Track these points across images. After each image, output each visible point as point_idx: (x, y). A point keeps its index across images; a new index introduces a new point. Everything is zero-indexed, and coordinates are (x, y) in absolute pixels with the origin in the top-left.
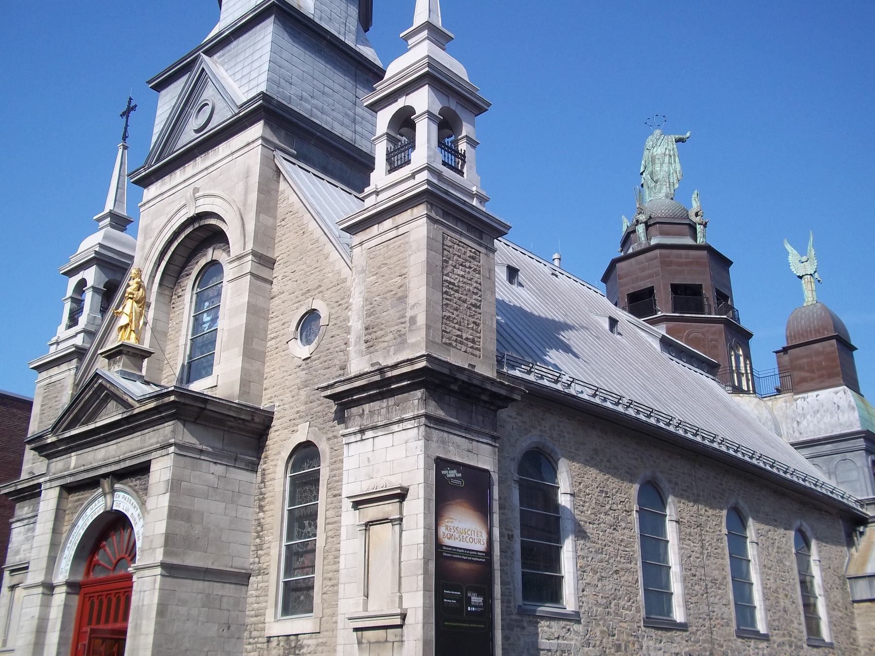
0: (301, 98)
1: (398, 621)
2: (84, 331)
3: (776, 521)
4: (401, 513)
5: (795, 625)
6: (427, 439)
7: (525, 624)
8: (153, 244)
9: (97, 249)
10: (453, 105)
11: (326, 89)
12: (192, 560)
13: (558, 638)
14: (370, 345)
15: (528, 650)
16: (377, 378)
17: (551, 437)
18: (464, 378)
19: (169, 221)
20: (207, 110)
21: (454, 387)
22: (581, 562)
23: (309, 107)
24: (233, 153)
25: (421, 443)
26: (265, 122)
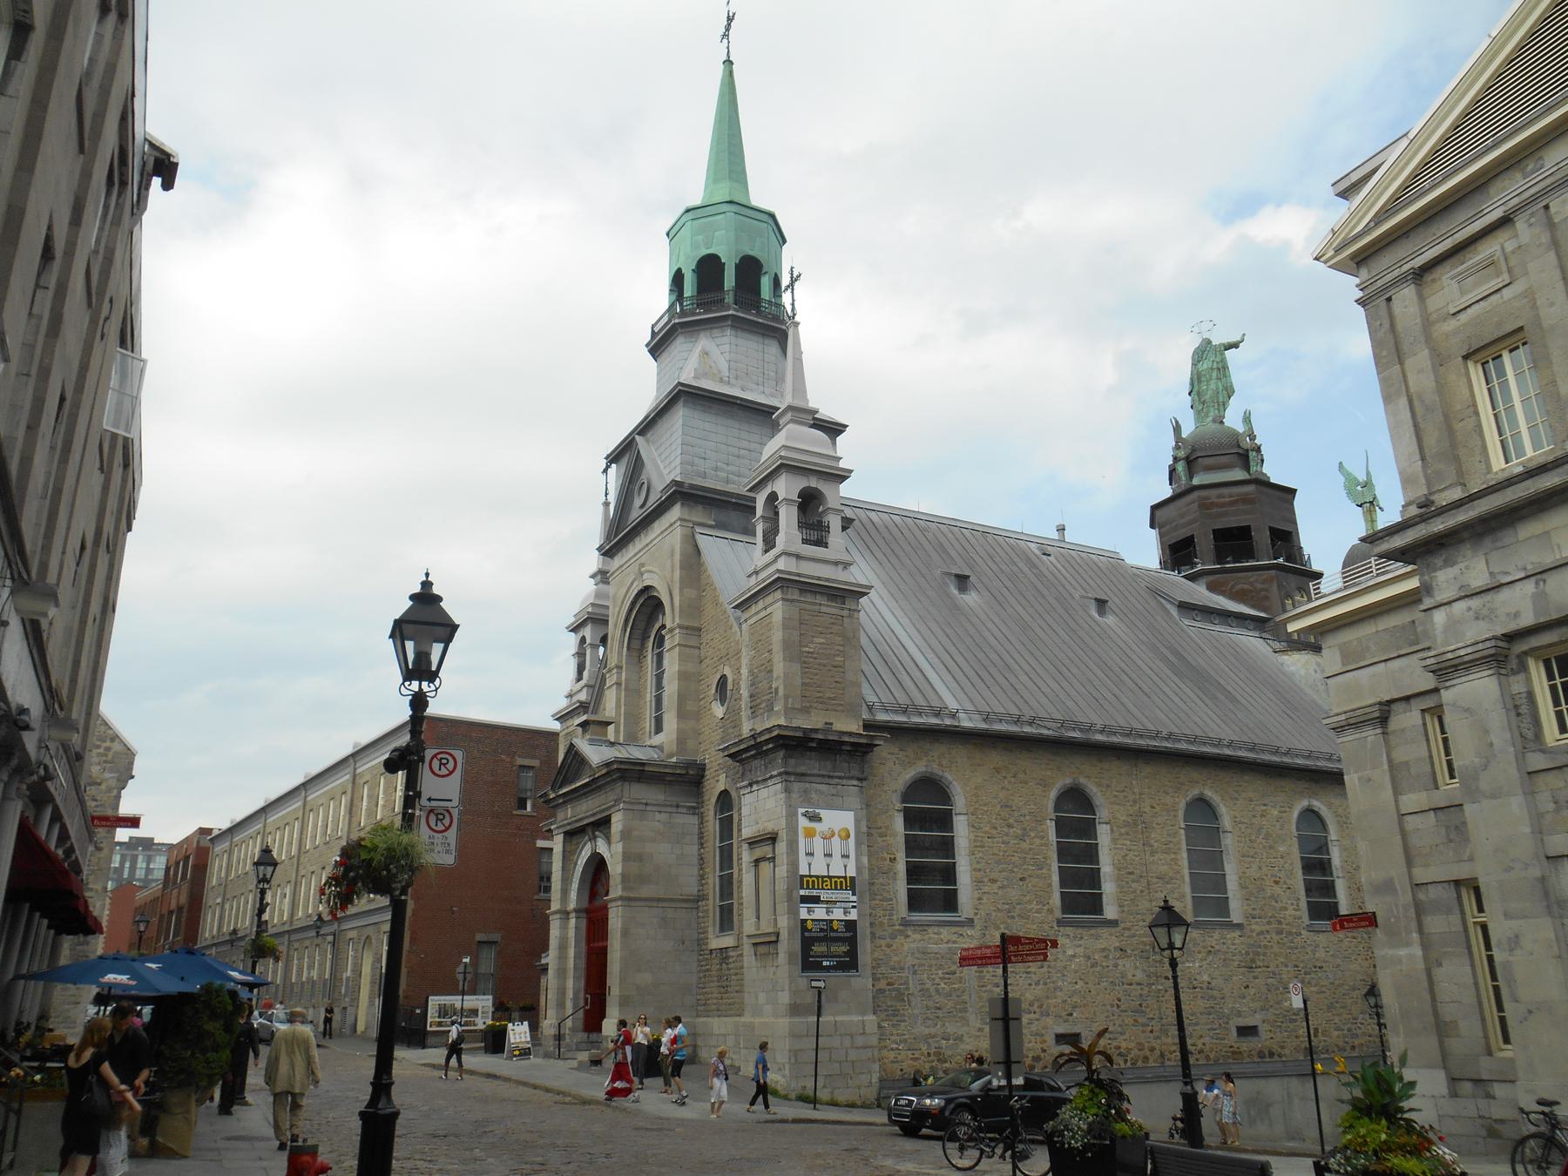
0: (716, 469)
1: (773, 939)
2: (586, 686)
3: (1265, 805)
4: (774, 853)
5: (1290, 912)
6: (787, 790)
7: (909, 933)
8: (619, 613)
9: (590, 610)
10: (813, 483)
11: (742, 452)
12: (645, 891)
13: (947, 943)
14: (754, 710)
15: (913, 954)
16: (752, 743)
17: (940, 765)
18: (820, 736)
19: (627, 592)
20: (645, 486)
21: (814, 745)
22: (979, 874)
23: (724, 475)
24: (662, 532)
25: (783, 795)
26: (682, 504)
